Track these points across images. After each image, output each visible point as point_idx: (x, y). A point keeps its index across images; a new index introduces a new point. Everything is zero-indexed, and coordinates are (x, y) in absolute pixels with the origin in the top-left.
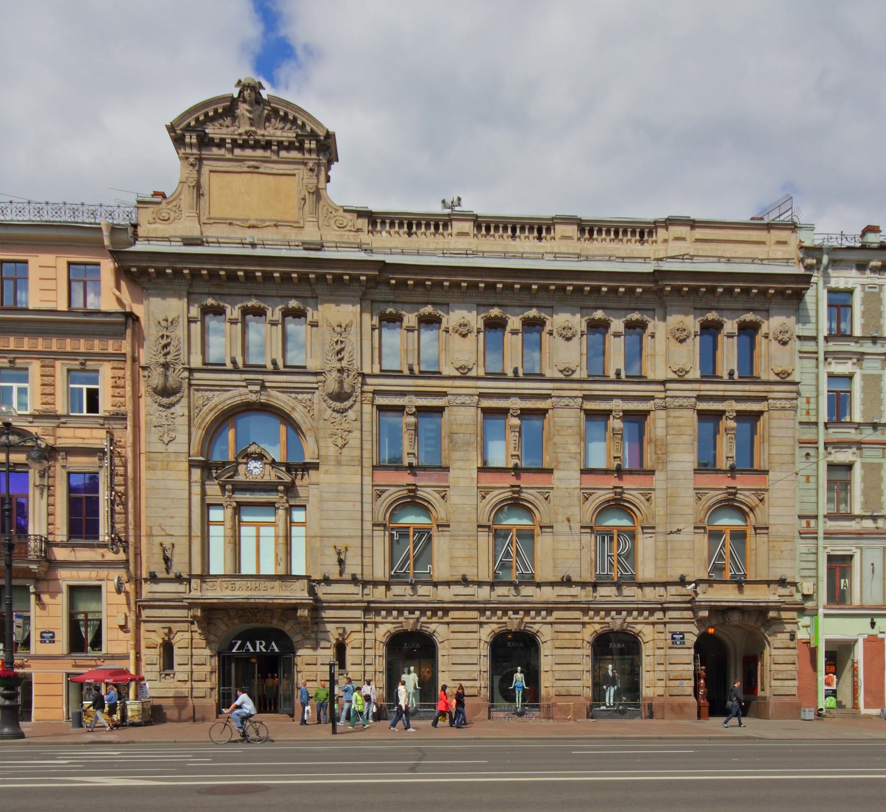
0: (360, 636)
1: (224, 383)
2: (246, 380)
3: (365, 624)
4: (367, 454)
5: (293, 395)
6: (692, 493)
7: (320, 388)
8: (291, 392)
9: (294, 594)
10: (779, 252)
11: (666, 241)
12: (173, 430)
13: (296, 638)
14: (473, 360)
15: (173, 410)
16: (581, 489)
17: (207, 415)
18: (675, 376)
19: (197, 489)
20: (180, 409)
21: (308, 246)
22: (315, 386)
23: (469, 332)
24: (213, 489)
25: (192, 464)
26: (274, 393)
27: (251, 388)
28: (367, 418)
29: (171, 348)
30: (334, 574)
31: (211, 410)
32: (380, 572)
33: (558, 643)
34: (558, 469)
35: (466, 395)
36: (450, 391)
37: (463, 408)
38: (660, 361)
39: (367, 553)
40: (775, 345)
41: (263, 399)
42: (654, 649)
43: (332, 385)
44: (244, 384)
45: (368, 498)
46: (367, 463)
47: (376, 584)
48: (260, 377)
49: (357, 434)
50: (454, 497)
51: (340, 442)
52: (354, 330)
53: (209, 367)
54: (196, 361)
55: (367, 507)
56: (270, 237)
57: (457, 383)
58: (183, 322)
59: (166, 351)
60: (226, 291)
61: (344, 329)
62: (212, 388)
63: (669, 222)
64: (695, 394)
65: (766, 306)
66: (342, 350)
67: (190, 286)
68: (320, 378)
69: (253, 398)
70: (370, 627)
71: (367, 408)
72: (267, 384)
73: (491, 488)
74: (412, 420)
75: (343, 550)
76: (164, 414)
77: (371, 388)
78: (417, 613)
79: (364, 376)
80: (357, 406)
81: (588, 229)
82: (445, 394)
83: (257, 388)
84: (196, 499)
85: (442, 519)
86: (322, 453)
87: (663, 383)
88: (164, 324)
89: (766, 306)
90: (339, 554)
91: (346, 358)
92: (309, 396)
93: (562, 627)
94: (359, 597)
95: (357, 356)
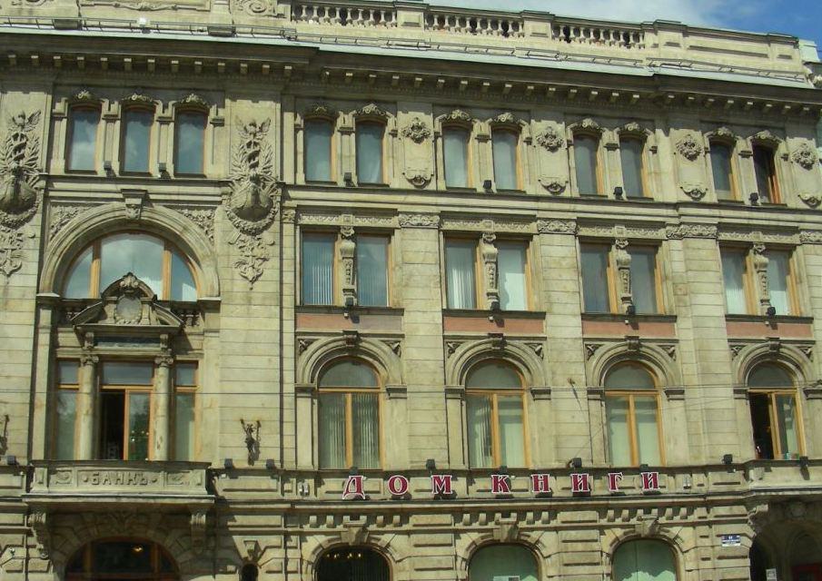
0: (279, 553)
1: (92, 195)
2: (123, 190)
3: (287, 536)
4: (288, 290)
5: (186, 211)
6: (726, 345)
7: (224, 202)
8: (183, 208)
9: (185, 491)
10: (786, 65)
11: (656, 46)
12: (19, 257)
13: (182, 559)
14: (432, 170)
15: (20, 230)
16: (584, 339)
17: (67, 236)
18: (688, 199)
19: (44, 338)
20: (31, 229)
21: (213, 30)
22: (218, 199)
23: (425, 136)
24: (68, 338)
25: (41, 303)
26: (159, 208)
27: (129, 201)
28: (288, 241)
29: (27, 151)
30: (240, 458)
31: (73, 231)
32: (306, 460)
33: (567, 558)
34: (552, 313)
35: (423, 214)
36: (400, 208)
37: (419, 231)
38: (668, 179)
39: (288, 429)
40: (797, 168)
41: (146, 216)
42: (696, 559)
43: (242, 196)
44: (121, 196)
45: (289, 351)
46: (288, 302)
47: (301, 475)
48: (143, 187)
49: (275, 262)
50: (410, 350)
51: (250, 274)
52: (273, 130)
53: (71, 176)
54: (58, 167)
55: (288, 364)
56: (166, 20)
57: (411, 198)
58: (44, 122)
59: (18, 154)
60: (105, 81)
61: (258, 128)
62: (75, 202)
63: (658, 26)
64: (716, 221)
65: (781, 125)
66: (256, 154)
67: (59, 76)
68: (227, 189)
69: (132, 213)
70: (294, 540)
71: (288, 229)
72: (152, 197)
73: (462, 337)
74: (350, 245)
75: (255, 425)
76: (9, 235)
77: (294, 203)
78: (363, 519)
79: (284, 187)
80: (276, 224)
81: (564, 28)
82: (395, 213)
83: (138, 201)
84: (43, 353)
85: (395, 381)
86: (226, 287)
87: (676, 206)
88: (20, 120)
89: (781, 125)
90: (250, 430)
91: (261, 165)
92: (209, 213)
93: (573, 534)
94: (278, 495)
95: (275, 162)
